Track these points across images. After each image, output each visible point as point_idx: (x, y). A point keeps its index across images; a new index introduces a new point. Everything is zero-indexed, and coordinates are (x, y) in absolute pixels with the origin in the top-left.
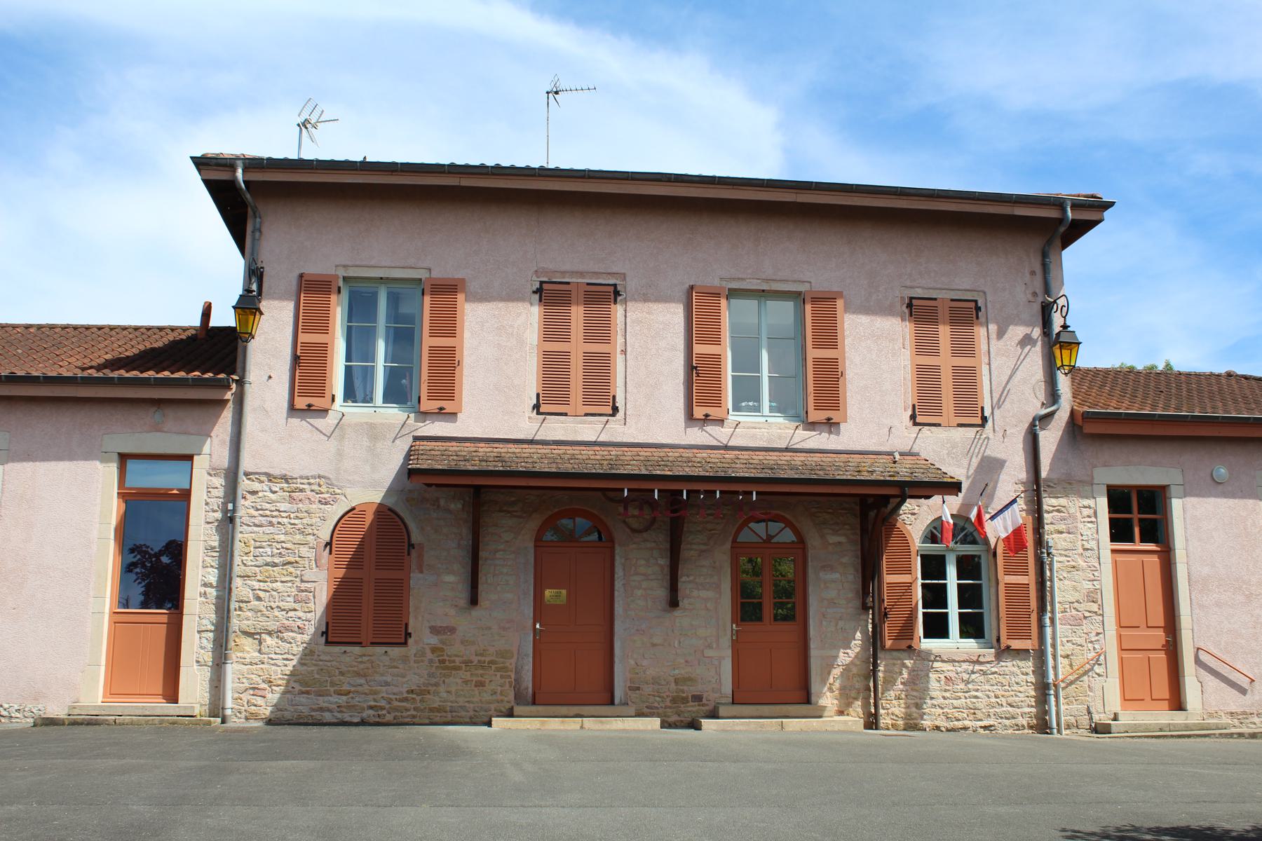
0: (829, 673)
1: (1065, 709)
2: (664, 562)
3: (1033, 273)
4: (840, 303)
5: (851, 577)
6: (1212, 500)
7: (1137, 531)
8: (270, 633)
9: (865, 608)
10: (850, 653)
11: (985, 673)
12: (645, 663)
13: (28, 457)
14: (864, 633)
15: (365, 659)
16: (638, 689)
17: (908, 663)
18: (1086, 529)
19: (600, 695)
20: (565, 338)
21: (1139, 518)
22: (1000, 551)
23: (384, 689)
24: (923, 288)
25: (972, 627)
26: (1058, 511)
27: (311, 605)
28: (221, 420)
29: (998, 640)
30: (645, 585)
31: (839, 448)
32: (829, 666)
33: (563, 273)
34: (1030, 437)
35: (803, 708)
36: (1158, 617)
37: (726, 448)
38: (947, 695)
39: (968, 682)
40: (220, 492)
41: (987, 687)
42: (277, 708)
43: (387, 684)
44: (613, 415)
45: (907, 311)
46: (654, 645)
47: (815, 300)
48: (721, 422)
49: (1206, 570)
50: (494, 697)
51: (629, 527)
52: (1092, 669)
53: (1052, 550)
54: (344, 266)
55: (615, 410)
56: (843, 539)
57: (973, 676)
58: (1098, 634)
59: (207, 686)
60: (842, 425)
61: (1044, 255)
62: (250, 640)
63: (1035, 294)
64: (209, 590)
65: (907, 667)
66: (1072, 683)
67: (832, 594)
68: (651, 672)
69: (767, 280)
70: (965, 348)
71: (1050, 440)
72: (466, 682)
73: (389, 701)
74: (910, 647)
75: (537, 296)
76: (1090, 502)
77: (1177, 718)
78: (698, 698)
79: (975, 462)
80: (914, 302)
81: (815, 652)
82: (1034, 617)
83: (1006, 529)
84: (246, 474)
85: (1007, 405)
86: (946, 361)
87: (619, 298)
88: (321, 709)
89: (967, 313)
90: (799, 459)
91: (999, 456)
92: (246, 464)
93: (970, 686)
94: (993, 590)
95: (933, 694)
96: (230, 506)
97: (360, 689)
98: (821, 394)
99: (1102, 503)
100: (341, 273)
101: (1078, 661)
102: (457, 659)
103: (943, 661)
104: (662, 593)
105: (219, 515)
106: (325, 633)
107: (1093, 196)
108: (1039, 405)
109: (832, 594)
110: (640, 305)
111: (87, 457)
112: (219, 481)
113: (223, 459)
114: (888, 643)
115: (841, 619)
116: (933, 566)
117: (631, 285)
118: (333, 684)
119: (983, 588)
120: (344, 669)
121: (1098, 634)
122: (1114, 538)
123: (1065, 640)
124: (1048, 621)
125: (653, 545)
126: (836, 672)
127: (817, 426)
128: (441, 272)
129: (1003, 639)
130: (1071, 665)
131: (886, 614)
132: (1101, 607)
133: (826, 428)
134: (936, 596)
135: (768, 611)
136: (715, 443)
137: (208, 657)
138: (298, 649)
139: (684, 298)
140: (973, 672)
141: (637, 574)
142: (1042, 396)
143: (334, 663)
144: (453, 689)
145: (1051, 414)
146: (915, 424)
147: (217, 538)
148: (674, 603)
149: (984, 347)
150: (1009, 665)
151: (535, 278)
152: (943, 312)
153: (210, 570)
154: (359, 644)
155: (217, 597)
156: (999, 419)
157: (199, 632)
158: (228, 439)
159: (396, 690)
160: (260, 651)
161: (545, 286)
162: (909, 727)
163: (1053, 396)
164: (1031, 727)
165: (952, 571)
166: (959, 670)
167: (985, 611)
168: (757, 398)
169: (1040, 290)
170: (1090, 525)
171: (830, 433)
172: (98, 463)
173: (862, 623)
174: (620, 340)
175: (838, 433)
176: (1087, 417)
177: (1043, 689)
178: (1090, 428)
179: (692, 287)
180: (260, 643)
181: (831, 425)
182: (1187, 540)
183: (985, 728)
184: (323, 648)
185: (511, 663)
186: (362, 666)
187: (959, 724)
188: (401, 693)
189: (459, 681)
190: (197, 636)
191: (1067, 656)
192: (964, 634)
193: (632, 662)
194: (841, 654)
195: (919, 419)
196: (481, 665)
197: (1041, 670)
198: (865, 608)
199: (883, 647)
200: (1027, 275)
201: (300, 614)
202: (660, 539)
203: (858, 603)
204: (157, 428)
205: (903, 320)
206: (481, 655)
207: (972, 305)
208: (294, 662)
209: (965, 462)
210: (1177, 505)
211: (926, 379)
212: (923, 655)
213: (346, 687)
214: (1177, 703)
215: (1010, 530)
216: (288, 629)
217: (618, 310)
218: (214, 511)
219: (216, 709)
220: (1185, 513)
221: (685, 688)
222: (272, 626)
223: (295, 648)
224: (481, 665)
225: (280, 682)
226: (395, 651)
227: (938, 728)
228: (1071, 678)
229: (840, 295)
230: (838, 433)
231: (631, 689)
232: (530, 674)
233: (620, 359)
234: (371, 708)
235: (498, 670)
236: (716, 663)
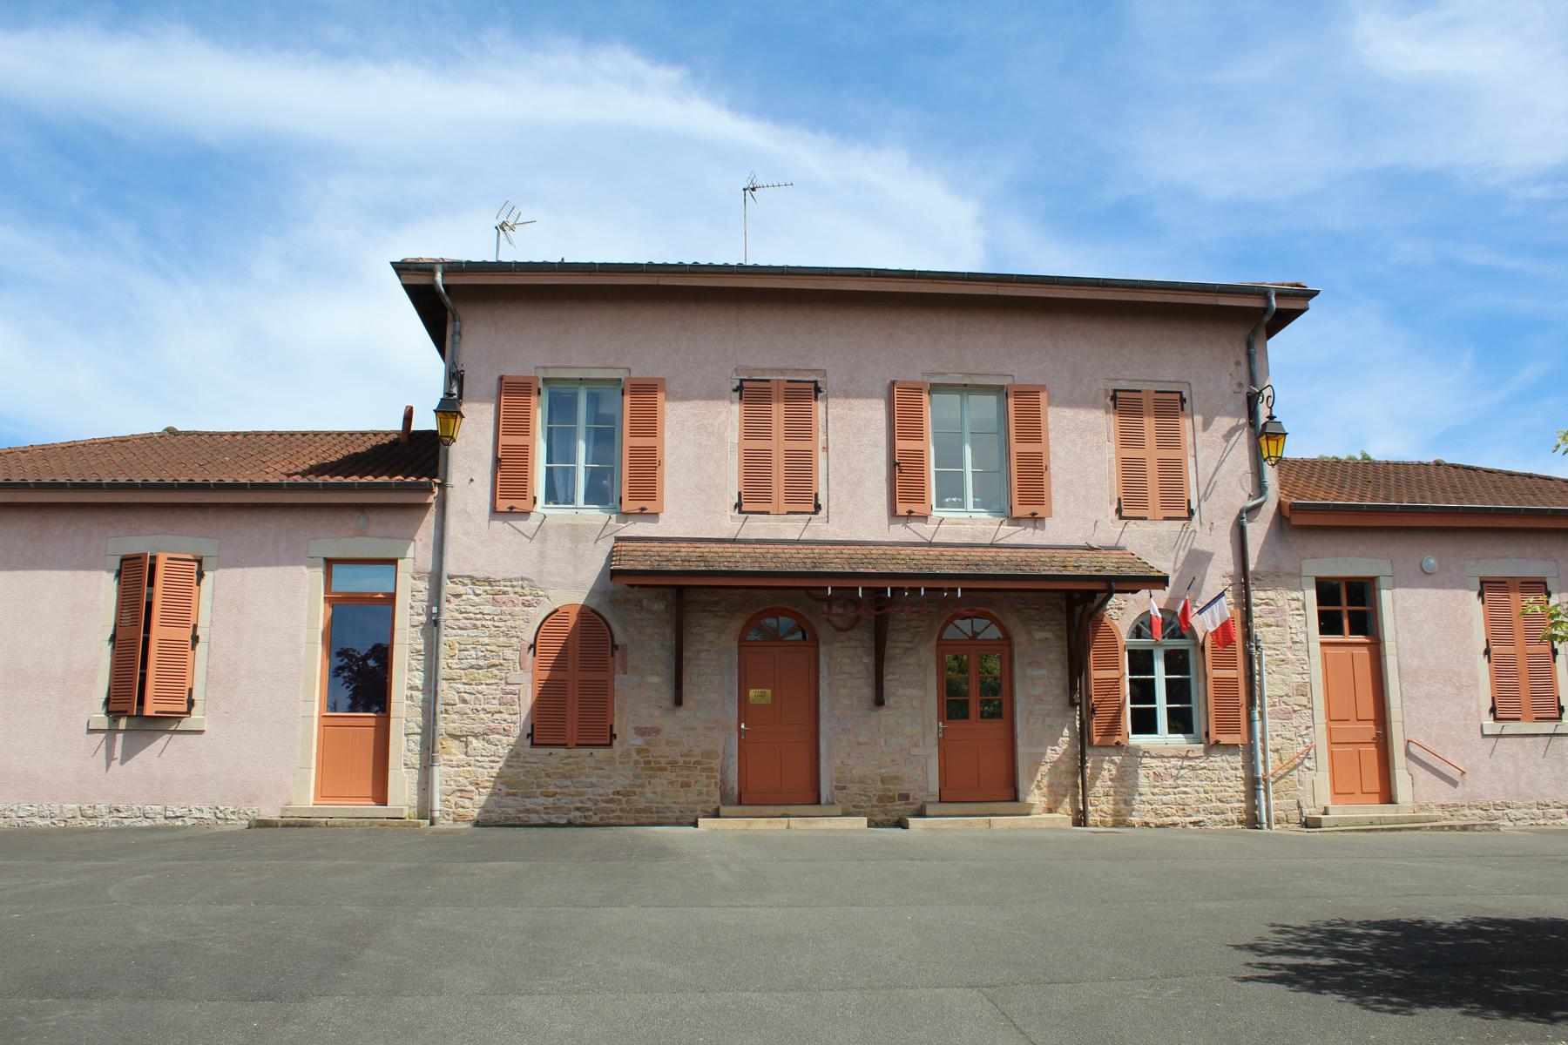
1: (1274, 804)
2: (869, 660)
3: (1238, 363)
4: (1043, 396)
5: (1058, 674)
6: (1422, 591)
7: (1346, 623)
8: (476, 736)
9: (1072, 704)
10: (1059, 749)
11: (1193, 769)
13: (238, 563)
14: (1073, 729)
17: (1117, 759)
18: (1295, 622)
19: (807, 794)
20: (767, 436)
21: (1348, 609)
22: (1208, 645)
25: (1181, 722)
27: (516, 707)
28: (424, 524)
29: (1207, 734)
32: (1037, 762)
33: (764, 371)
36: (1368, 710)
37: (930, 544)
40: (425, 596)
42: (484, 809)
43: (593, 785)
44: (816, 513)
46: (860, 744)
47: (1017, 393)
48: (924, 518)
49: (1415, 662)
55: (818, 507)
56: (1049, 635)
59: (415, 788)
60: (1047, 520)
61: (1249, 345)
63: (1240, 385)
64: (415, 693)
66: (1281, 777)
67: (1039, 690)
69: (969, 375)
70: (1170, 440)
71: (1257, 532)
72: (672, 783)
73: (596, 802)
76: (1299, 595)
77: (1388, 811)
78: (904, 797)
79: (1182, 555)
81: (1022, 749)
82: (1243, 711)
83: (1214, 623)
84: (450, 577)
85: (1214, 497)
86: (1151, 453)
88: (528, 811)
89: (1172, 405)
90: (1004, 554)
92: (450, 567)
94: (1201, 685)
95: (1142, 790)
96: (435, 610)
98: (1024, 489)
99: (1312, 595)
100: (541, 374)
102: (663, 760)
104: (867, 691)
105: (423, 619)
109: (1039, 690)
110: (841, 401)
111: (295, 562)
112: (423, 585)
114: (1096, 740)
116: (1142, 661)
117: (832, 381)
118: (539, 786)
119: (1190, 683)
120: (550, 771)
122: (1323, 631)
124: (1257, 716)
126: (1044, 769)
129: (1212, 733)
132: (1311, 700)
133: (1031, 522)
134: (1143, 691)
135: (974, 708)
136: (919, 540)
137: (415, 760)
138: (504, 751)
139: (885, 393)
142: (1249, 487)
144: (659, 790)
145: (1258, 506)
146: (1121, 518)
148: (879, 701)
149: (1190, 439)
150: (1218, 760)
152: (1148, 404)
155: (424, 700)
156: (1205, 511)
158: (431, 542)
159: (601, 791)
160: (466, 754)
162: (1116, 824)
163: (1260, 488)
164: (1241, 822)
165: (1159, 666)
167: (1193, 705)
168: (961, 493)
169: (1245, 380)
171: (1035, 528)
174: (822, 437)
175: (1043, 528)
176: (1295, 508)
177: (1253, 784)
178: (1297, 520)
179: (893, 383)
181: (1035, 520)
183: (1195, 823)
184: (529, 750)
185: (716, 764)
196: (686, 766)
197: (1250, 765)
198: (1072, 704)
199: (1091, 743)
200: (1232, 361)
201: (505, 716)
202: (865, 636)
203: (1065, 699)
204: (362, 533)
209: (1172, 556)
210: (1386, 597)
211: (1131, 472)
213: (552, 789)
214: (1388, 797)
216: (493, 731)
217: (819, 407)
219: (425, 811)
220: (1392, 604)
222: (478, 728)
224: (686, 766)
226: (600, 753)
227: (1147, 824)
229: (1043, 388)
230: (1043, 528)
231: (837, 788)
233: (821, 456)
234: (578, 809)
235: (703, 770)
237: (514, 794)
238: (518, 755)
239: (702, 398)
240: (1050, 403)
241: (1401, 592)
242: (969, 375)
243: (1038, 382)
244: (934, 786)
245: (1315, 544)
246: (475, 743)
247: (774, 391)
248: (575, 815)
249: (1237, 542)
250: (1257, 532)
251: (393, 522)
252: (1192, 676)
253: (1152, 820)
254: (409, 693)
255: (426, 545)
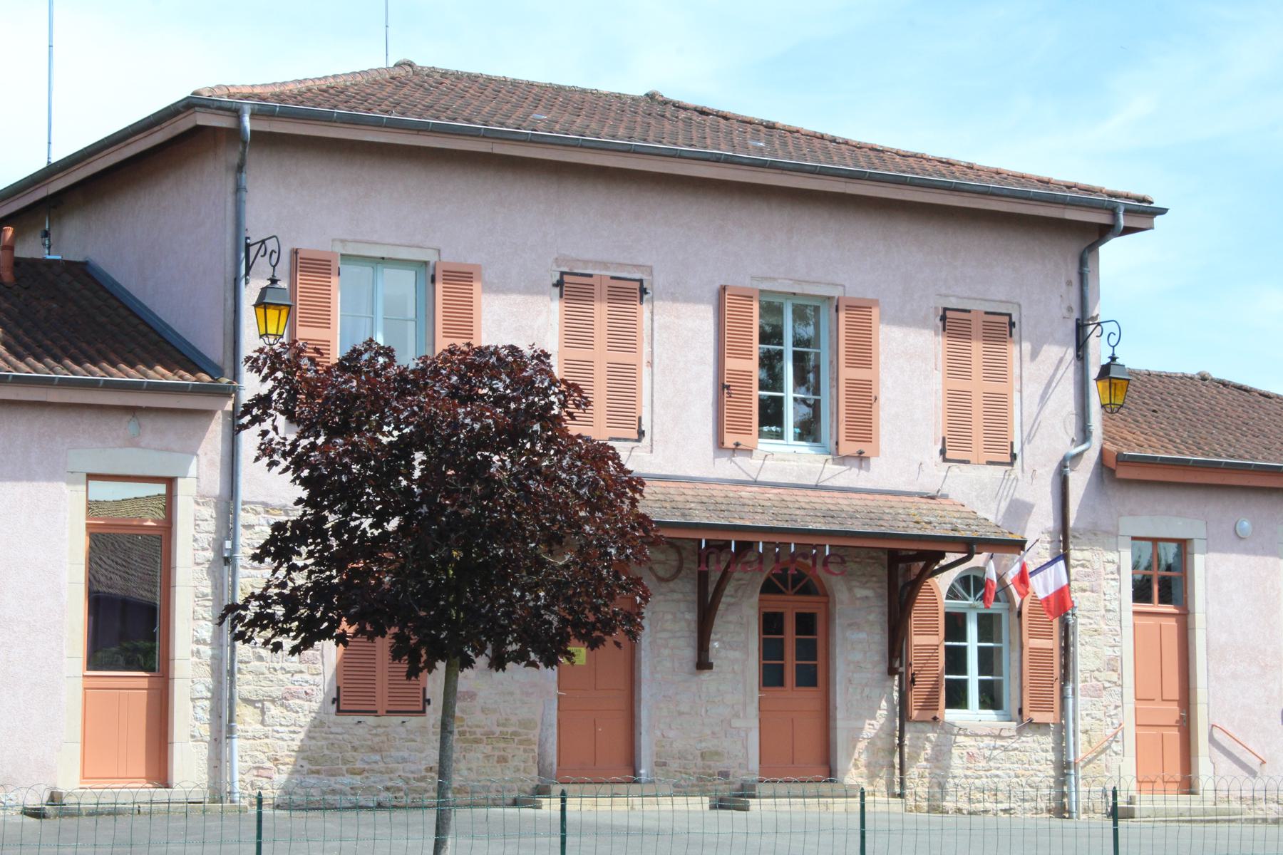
0: (854, 747)
1: (1085, 792)
2: (692, 616)
3: (1069, 283)
4: (875, 312)
5: (877, 638)
6: (1233, 556)
7: (1156, 588)
8: (273, 701)
9: (892, 671)
10: (877, 722)
11: (1006, 749)
12: (671, 734)
14: (890, 701)
15: (380, 730)
16: (664, 764)
17: (932, 736)
18: (1109, 587)
19: (626, 769)
20: (587, 343)
22: (1025, 610)
23: (401, 766)
24: (958, 297)
25: (991, 698)
26: (1083, 566)
27: (319, 666)
28: (209, 435)
29: (1020, 711)
30: (672, 642)
31: (869, 486)
32: (854, 740)
33: (586, 262)
34: (1058, 480)
35: (825, 788)
36: (1173, 691)
37: (755, 483)
38: (969, 773)
39: (989, 759)
40: (211, 526)
41: (1008, 765)
42: (287, 791)
43: (404, 760)
44: (639, 440)
45: (940, 324)
46: (680, 714)
48: (749, 451)
50: (517, 775)
51: (656, 576)
52: (1109, 747)
53: (1077, 612)
54: (343, 241)
55: (641, 433)
56: (869, 593)
57: (995, 752)
58: (1116, 707)
59: (204, 766)
60: (873, 460)
61: (1082, 263)
62: (251, 708)
63: (1070, 309)
64: (202, 648)
65: (930, 741)
66: (1090, 762)
68: (678, 745)
69: (799, 282)
70: (997, 371)
71: (1079, 480)
72: (488, 757)
73: (407, 781)
74: (935, 718)
75: (557, 290)
77: (1184, 802)
78: (725, 775)
79: (1004, 505)
80: (949, 314)
82: (1057, 686)
83: (1046, 588)
84: (244, 503)
85: (1036, 441)
86: (977, 385)
87: (645, 297)
88: (334, 792)
89: (1002, 328)
90: (827, 500)
91: (1027, 500)
92: (244, 493)
93: (992, 764)
94: (1016, 655)
95: (957, 772)
96: (228, 544)
97: (375, 767)
99: (1126, 558)
100: (339, 249)
101: (1097, 737)
102: (478, 731)
103: (966, 735)
104: (690, 653)
105: (210, 555)
106: (336, 700)
107: (1143, 200)
108: (1069, 441)
109: (858, 656)
110: (668, 305)
111: (52, 476)
112: (208, 512)
113: (214, 482)
114: (915, 714)
115: (866, 685)
116: (955, 626)
117: (657, 282)
118: (345, 762)
120: (357, 743)
121: (1116, 707)
123: (1084, 713)
124: (1070, 691)
125: (680, 596)
126: (862, 745)
127: (847, 460)
128: (453, 256)
129: (1025, 711)
130: (1089, 742)
131: (913, 681)
132: (1121, 676)
133: (856, 462)
134: (956, 660)
135: (790, 675)
136: (744, 477)
137: (205, 730)
138: (305, 720)
139: (714, 299)
140: (995, 748)
141: (664, 630)
142: (1072, 430)
143: (346, 736)
144: (474, 765)
145: (1080, 454)
146: (945, 460)
147: (209, 583)
148: (703, 663)
149: (1016, 371)
151: (554, 268)
152: (977, 327)
153: (202, 623)
154: (374, 712)
155: (213, 657)
156: (1028, 456)
157: (193, 700)
158: (218, 459)
159: (414, 767)
160: (263, 723)
161: (566, 278)
162: (932, 809)
163: (1084, 433)
164: (1049, 811)
165: (972, 629)
166: (982, 745)
167: (1005, 678)
170: (1113, 583)
171: (860, 467)
172: (63, 485)
173: (888, 690)
174: (646, 349)
175: (868, 469)
176: (1122, 460)
177: (1064, 768)
178: (1122, 473)
179: (724, 288)
180: (263, 712)
181: (861, 458)
182: (1207, 603)
183: (1005, 811)
184: (333, 718)
185: (534, 735)
186: (377, 739)
187: (980, 807)
188: (420, 771)
189: (481, 756)
190: (191, 704)
191: (1086, 732)
192: (984, 704)
193: (658, 733)
194: (867, 726)
195: (949, 455)
197: (1061, 747)
198: (892, 671)
199: (909, 719)
200: (1064, 284)
201: (307, 677)
203: (884, 667)
204: (133, 443)
205: (936, 334)
206: (504, 725)
207: (1006, 319)
208: (302, 736)
209: (993, 506)
210: (1201, 563)
211: (957, 403)
212: (946, 727)
213: (359, 765)
214: (1188, 786)
215: (1051, 590)
216: (294, 695)
217: (644, 310)
218: (204, 549)
219: (218, 793)
220: (1216, 577)
221: (712, 763)
222: (276, 691)
223: (303, 719)
225: (287, 760)
226: (413, 721)
227: (959, 811)
228: (1090, 757)
229: (875, 303)
230: (868, 469)
231: (657, 764)
232: (555, 747)
233: (646, 371)
234: (387, 789)
235: (521, 742)
236: (743, 734)
237: (318, 772)
238: (322, 723)
239: (520, 292)
240: (881, 320)
241: (1214, 557)
242: (799, 282)
243: (870, 296)
244: (754, 764)
245: (1135, 499)
246: (274, 710)
247: (597, 288)
248: (384, 797)
249: (1058, 495)
250: (1079, 480)
251: (172, 430)
252: (1004, 645)
253: (964, 806)
254: (195, 647)
255: (211, 463)
